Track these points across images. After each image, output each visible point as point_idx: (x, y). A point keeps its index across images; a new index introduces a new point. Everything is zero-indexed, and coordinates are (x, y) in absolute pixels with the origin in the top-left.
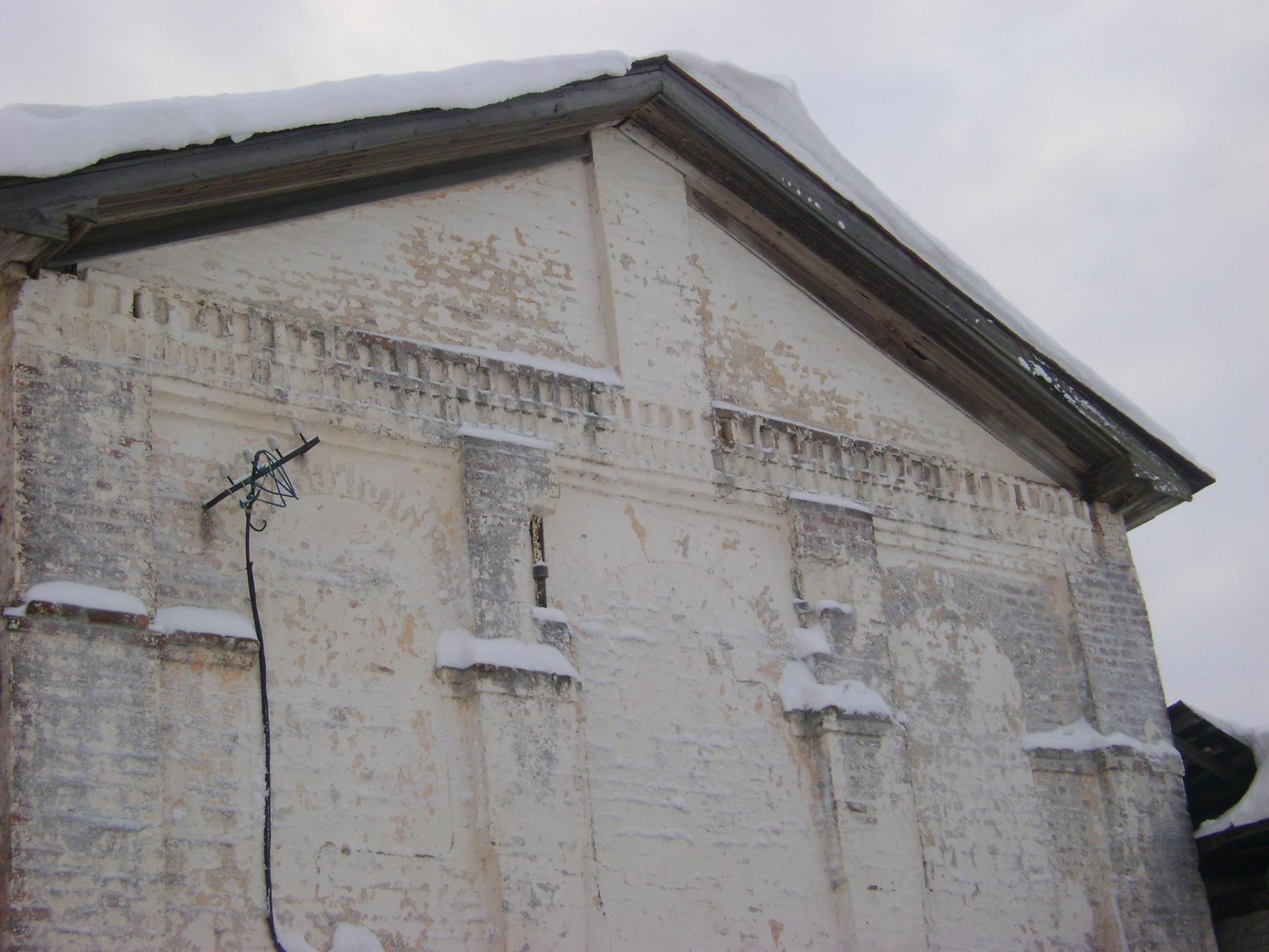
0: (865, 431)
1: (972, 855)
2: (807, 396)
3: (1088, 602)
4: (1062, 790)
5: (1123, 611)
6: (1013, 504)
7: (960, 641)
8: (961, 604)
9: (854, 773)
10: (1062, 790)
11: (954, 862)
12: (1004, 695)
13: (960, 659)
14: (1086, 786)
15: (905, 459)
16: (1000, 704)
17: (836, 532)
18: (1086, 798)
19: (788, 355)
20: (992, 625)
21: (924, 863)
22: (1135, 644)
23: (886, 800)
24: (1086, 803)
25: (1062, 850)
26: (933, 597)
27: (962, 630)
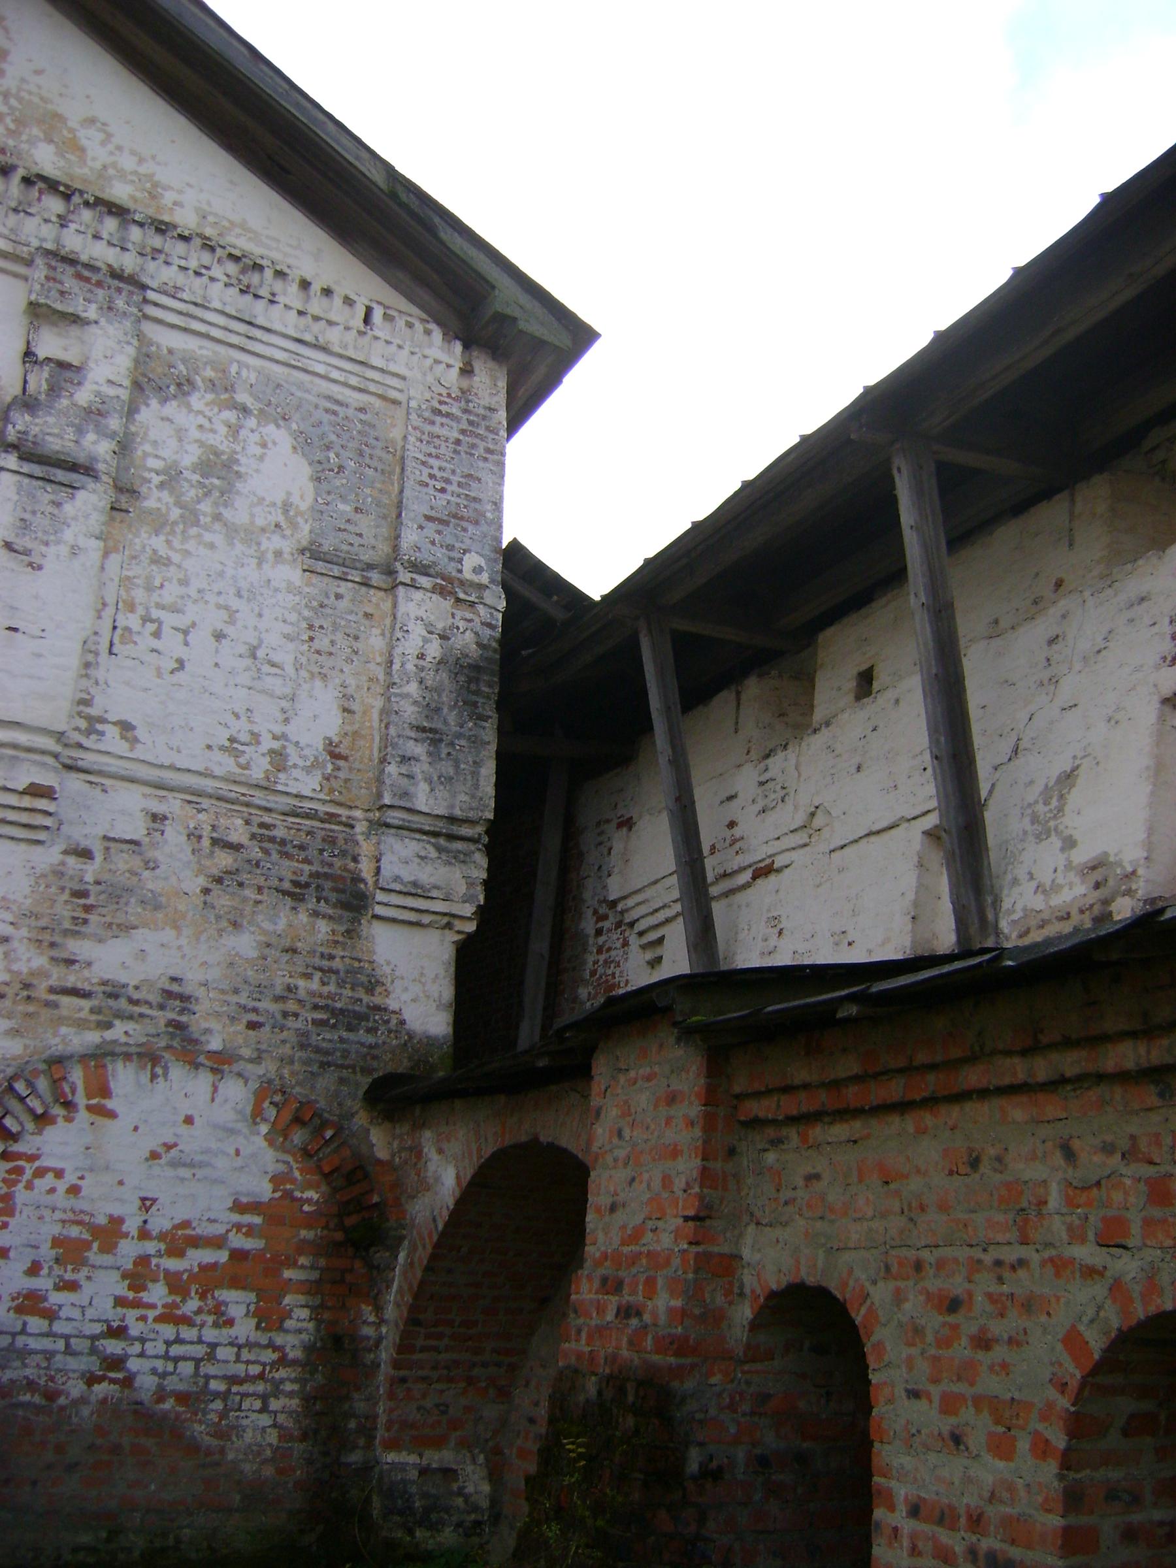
0: (186, 219)
1: (186, 633)
2: (111, 171)
3: (428, 428)
4: (338, 597)
5: (474, 446)
6: (358, 322)
7: (243, 433)
8: (257, 399)
9: (27, 516)
10: (338, 597)
11: (157, 634)
12: (289, 494)
13: (238, 449)
14: (374, 600)
15: (219, 250)
16: (279, 498)
17: (91, 291)
18: (369, 611)
19: (100, 130)
20: (294, 426)
21: (115, 628)
22: (479, 480)
23: (64, 550)
24: (367, 616)
25: (318, 652)
26: (223, 387)
27: (252, 422)
